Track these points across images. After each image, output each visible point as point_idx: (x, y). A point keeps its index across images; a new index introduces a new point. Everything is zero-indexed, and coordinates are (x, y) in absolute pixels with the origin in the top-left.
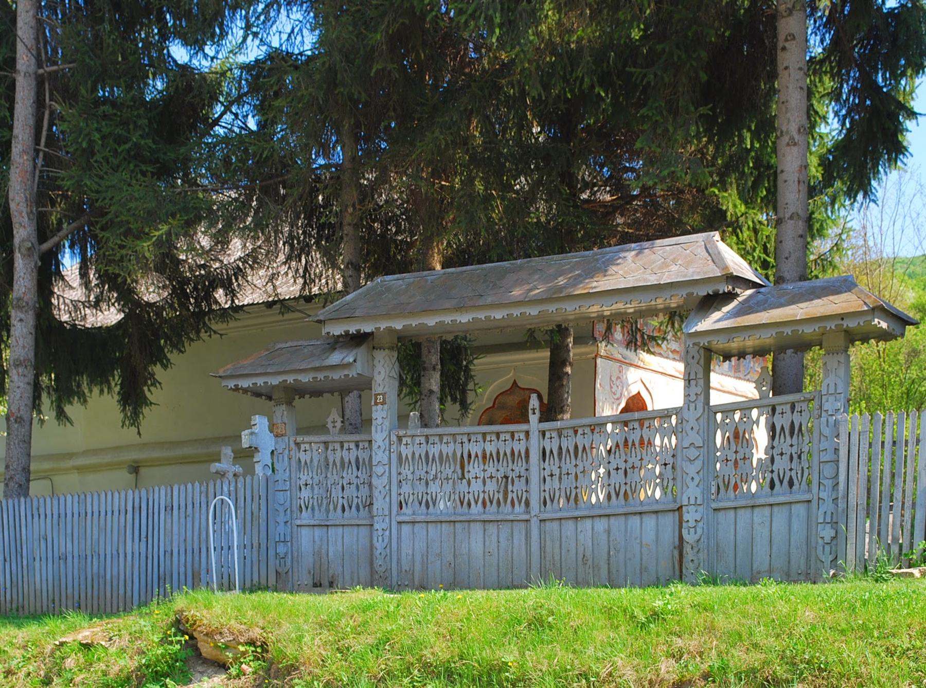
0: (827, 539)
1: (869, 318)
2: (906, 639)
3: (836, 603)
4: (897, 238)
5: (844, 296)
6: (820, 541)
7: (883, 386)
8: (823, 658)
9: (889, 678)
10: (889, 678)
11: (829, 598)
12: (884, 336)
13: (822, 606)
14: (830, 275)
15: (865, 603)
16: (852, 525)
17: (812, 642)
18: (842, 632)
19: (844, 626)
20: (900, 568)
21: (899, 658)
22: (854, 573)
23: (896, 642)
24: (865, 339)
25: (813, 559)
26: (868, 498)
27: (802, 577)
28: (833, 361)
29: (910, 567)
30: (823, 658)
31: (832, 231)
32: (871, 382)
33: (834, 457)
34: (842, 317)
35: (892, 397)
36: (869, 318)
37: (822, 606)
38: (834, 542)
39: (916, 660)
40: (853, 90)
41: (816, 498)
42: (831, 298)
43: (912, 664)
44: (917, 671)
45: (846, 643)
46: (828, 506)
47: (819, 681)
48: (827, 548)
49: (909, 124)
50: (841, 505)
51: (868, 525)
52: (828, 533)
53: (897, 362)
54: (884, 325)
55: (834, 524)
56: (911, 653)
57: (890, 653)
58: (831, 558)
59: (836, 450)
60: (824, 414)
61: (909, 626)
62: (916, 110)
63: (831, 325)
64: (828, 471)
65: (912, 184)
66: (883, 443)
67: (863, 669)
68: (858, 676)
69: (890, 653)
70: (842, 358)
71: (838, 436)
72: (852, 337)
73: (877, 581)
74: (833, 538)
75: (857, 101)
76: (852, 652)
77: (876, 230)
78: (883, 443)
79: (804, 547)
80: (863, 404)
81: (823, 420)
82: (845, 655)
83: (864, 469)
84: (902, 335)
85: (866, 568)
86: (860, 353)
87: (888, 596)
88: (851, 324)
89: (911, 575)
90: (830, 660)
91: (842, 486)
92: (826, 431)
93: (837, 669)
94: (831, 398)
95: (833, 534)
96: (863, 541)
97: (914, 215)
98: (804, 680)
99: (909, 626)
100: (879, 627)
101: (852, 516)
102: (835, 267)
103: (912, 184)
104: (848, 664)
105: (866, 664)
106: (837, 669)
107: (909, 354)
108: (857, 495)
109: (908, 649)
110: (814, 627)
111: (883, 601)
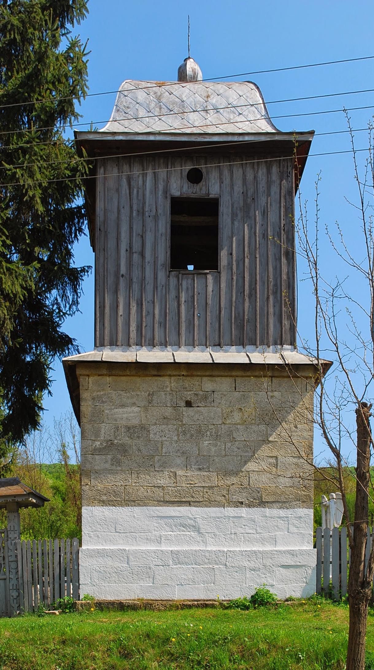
0: (15, 597)
1: (27, 497)
2: (52, 645)
3: (19, 628)
4: (41, 457)
5: (15, 487)
6: (11, 597)
7: (39, 523)
8: (14, 654)
9: (46, 663)
10: (46, 663)
11: (16, 626)
12: (34, 505)
13: (13, 629)
14: (9, 476)
15: (33, 628)
16: (26, 590)
17: (10, 647)
18: (23, 642)
19: (24, 639)
20: (49, 610)
21: (50, 654)
22: (28, 612)
23: (48, 646)
24: (26, 507)
25: (9, 605)
26: (33, 580)
27: (4, 614)
28: (12, 515)
29: (54, 610)
30: (14, 654)
31: (9, 455)
32: (34, 520)
33: (15, 559)
34: (15, 496)
35: (44, 528)
36: (27, 497)
37: (13, 629)
38: (18, 598)
39: (58, 655)
40: (12, 395)
41: (8, 578)
42: (9, 487)
43: (56, 656)
44: (59, 660)
45: (25, 647)
46: (14, 582)
47: (13, 665)
48: (15, 601)
49: (41, 413)
50: (21, 581)
51: (33, 589)
52: (15, 594)
53: (45, 513)
54: (34, 501)
55: (18, 590)
56: (55, 652)
57: (46, 651)
58: (17, 605)
59: (16, 556)
60: (9, 539)
61: (53, 639)
62: (43, 407)
63: (10, 499)
64: (13, 565)
65: (46, 434)
66: (38, 553)
67: (34, 659)
68: (32, 662)
69: (46, 651)
70: (16, 514)
71: (16, 550)
72: (20, 505)
73: (39, 616)
74: (17, 596)
75: (11, 412)
76: (27, 651)
77: (31, 453)
78: (38, 553)
79: (4, 600)
80: (31, 531)
81: (9, 542)
82: (25, 653)
83: (30, 565)
84: (43, 505)
85: (34, 610)
86: (24, 511)
87: (43, 625)
88: (20, 500)
89: (55, 613)
90: (18, 655)
91: (20, 573)
92: (11, 547)
93: (22, 659)
94: (12, 532)
95: (17, 594)
96: (35, 594)
97: (48, 448)
98: (6, 665)
99: (53, 639)
100: (40, 640)
101: (26, 586)
102: (11, 471)
103: (46, 434)
104: (27, 657)
105: (35, 657)
106: (22, 659)
107: (50, 509)
108: (27, 576)
109: (54, 650)
110: (9, 639)
111: (41, 627)
